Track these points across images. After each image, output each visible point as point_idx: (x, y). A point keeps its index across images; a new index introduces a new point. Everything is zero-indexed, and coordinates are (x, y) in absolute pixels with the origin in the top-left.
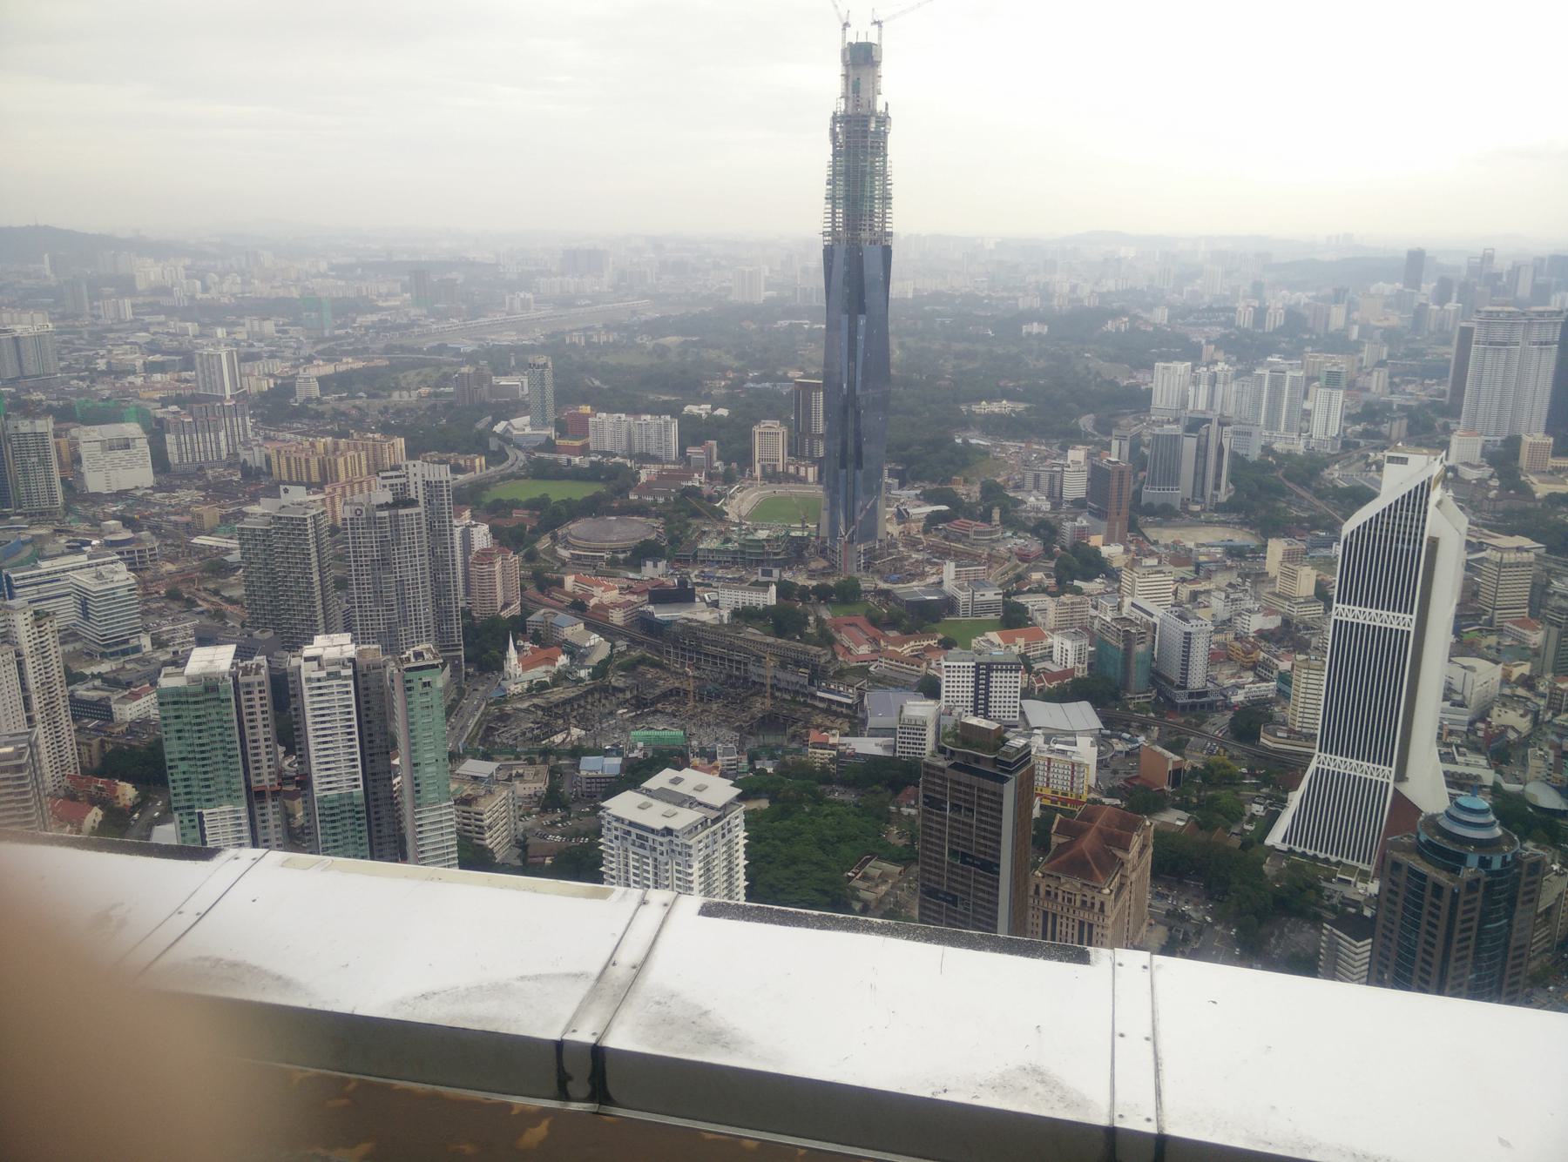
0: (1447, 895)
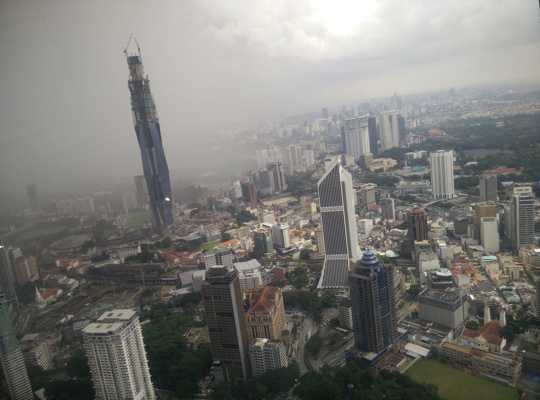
0: (368, 283)
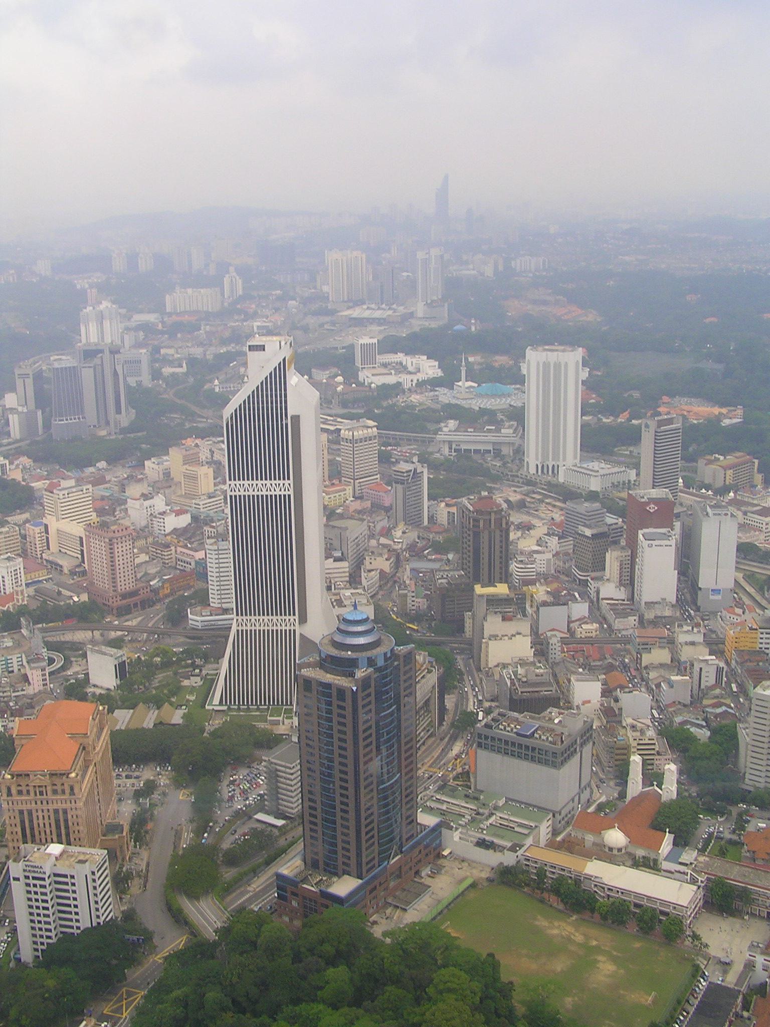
0: (348, 696)
